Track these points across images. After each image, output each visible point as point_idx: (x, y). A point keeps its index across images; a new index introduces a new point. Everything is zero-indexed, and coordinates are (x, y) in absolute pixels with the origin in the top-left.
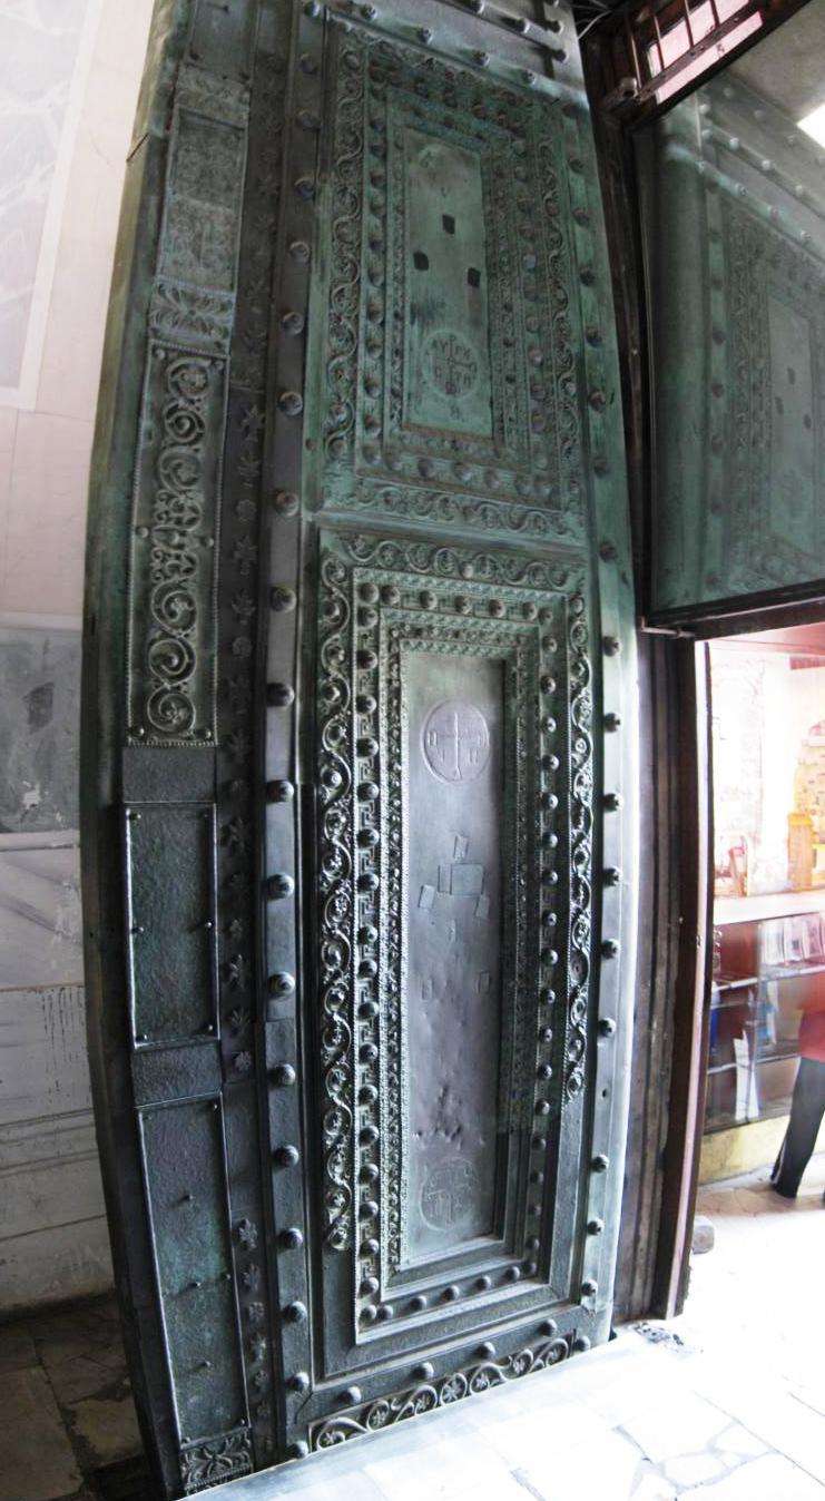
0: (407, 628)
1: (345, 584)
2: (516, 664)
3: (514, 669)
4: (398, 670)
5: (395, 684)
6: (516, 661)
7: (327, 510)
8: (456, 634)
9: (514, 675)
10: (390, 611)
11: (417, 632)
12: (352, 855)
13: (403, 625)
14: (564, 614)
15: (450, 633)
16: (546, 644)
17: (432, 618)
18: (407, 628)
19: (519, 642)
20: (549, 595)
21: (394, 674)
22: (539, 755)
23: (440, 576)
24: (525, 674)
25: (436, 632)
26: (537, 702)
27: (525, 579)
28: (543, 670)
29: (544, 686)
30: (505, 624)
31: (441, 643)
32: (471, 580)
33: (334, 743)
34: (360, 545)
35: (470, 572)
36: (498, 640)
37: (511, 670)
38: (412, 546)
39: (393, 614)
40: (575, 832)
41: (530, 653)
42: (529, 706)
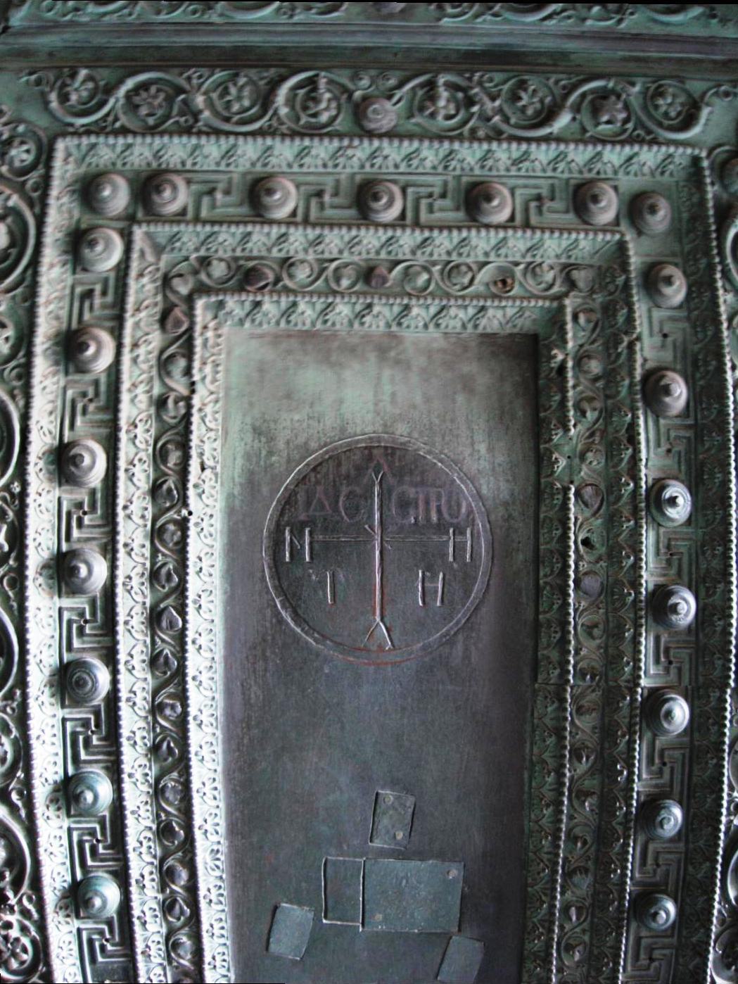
0: (219, 270)
1: (33, 178)
4: (188, 372)
5: (173, 411)
6: (563, 332)
7: (22, 33)
8: (368, 274)
9: (562, 368)
10: (163, 231)
13: (205, 262)
14: (702, 202)
15: (349, 271)
16: (652, 280)
17: (283, 237)
18: (219, 270)
19: (572, 284)
20: (649, 157)
21: (180, 387)
22: (635, 584)
23: (293, 134)
24: (595, 367)
25: (302, 274)
26: (633, 440)
27: (563, 121)
28: (648, 351)
29: (653, 389)
30: (518, 243)
31: (320, 303)
32: (391, 135)
34: (79, 90)
35: (386, 114)
36: (504, 281)
39: (174, 238)
41: (609, 310)
42: (612, 452)
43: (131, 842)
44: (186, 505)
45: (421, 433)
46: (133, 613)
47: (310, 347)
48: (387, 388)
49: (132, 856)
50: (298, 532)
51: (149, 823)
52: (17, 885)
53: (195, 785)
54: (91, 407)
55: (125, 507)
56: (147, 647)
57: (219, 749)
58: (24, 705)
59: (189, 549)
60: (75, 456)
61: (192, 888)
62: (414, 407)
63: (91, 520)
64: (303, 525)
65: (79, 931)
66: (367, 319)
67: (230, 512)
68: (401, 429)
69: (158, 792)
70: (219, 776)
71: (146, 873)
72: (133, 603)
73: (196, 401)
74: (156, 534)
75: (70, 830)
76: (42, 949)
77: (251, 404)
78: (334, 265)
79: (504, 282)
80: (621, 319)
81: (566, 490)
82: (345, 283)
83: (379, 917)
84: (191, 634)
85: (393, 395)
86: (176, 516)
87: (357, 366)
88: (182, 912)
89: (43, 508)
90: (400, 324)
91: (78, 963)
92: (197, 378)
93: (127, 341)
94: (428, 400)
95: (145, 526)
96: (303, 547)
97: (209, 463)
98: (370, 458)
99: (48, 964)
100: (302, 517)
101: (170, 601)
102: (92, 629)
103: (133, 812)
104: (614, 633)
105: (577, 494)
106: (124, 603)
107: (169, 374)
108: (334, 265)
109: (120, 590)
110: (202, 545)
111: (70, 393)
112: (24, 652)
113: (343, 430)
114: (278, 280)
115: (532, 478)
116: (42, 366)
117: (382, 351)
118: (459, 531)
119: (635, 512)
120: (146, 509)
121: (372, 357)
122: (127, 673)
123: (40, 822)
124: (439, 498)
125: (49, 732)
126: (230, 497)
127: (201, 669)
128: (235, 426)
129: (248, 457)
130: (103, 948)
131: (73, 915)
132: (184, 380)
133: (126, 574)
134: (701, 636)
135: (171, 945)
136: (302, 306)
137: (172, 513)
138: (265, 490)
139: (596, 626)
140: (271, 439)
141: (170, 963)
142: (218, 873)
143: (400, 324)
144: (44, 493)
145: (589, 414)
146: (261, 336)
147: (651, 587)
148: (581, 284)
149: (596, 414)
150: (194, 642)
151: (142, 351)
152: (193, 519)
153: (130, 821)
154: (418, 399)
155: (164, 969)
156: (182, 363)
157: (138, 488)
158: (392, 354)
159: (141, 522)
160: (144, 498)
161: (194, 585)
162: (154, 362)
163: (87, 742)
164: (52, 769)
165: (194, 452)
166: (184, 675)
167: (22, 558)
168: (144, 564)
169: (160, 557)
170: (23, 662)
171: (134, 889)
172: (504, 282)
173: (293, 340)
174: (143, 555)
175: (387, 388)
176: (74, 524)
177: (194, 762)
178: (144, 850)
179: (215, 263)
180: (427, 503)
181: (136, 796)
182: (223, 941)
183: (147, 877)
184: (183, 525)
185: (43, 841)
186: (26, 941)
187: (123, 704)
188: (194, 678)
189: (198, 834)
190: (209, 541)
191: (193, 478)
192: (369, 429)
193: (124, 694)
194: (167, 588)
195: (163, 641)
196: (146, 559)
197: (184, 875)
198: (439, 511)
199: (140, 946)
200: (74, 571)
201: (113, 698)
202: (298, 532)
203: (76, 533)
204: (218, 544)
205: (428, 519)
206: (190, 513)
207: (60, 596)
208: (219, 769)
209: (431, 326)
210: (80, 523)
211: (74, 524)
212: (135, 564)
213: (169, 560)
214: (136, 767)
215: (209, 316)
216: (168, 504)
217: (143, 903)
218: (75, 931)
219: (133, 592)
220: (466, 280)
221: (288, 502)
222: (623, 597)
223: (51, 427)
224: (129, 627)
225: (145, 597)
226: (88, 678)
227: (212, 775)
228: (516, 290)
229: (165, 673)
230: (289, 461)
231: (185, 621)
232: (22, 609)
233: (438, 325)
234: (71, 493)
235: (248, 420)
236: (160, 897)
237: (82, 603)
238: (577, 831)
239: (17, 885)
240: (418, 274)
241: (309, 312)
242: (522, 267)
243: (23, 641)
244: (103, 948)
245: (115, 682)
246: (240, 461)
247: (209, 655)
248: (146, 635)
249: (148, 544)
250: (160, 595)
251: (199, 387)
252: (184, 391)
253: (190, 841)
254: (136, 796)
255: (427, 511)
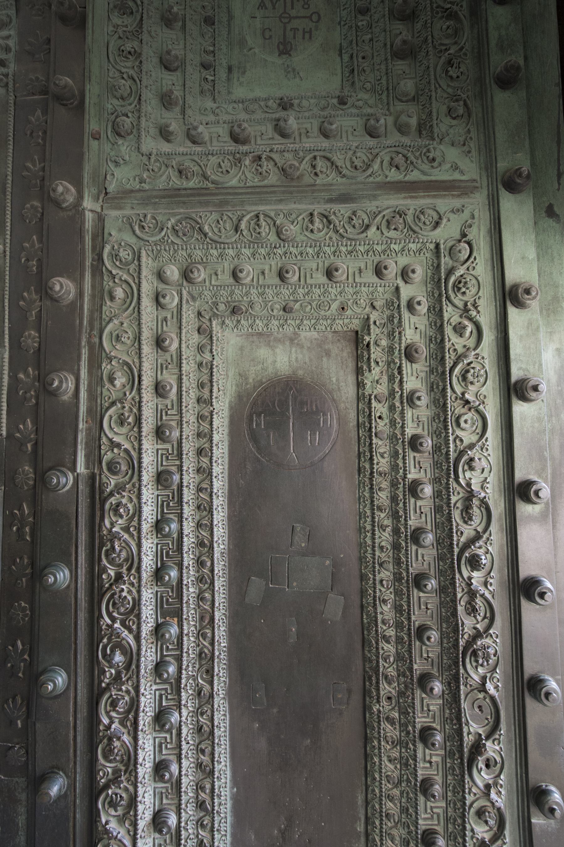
2: (369, 334)
3: (367, 338)
4: (211, 351)
6: (369, 330)
9: (368, 345)
11: (235, 311)
12: (139, 545)
13: (216, 304)
18: (222, 307)
21: (207, 356)
24: (384, 343)
25: (257, 308)
33: (124, 430)
37: (363, 340)
38: (215, 216)
40: (468, 531)
43: (185, 549)
44: (212, 405)
45: (308, 374)
47: (261, 340)
48: (294, 356)
49: (185, 555)
50: (259, 415)
51: (193, 540)
52: (129, 569)
53: (215, 522)
54: (170, 366)
55: (186, 407)
57: (226, 507)
58: (140, 490)
59: (214, 423)
60: (162, 386)
61: (212, 571)
62: (305, 363)
64: (262, 413)
65: (157, 592)
66: (285, 327)
67: (231, 408)
68: (300, 372)
69: (199, 525)
70: (226, 519)
71: (191, 563)
73: (215, 363)
74: (200, 417)
75: (157, 544)
76: (137, 603)
77: (238, 364)
78: (270, 304)
79: (343, 308)
80: (396, 321)
81: (370, 395)
82: (275, 311)
83: (295, 584)
84: (214, 459)
85: (297, 358)
87: (281, 347)
88: (206, 582)
90: (299, 328)
91: (154, 608)
92: (215, 353)
93: (183, 338)
94: (311, 360)
96: (261, 422)
97: (222, 388)
98: (288, 385)
99: (139, 610)
100: (260, 410)
101: (206, 445)
103: (186, 536)
104: (395, 455)
105: (375, 397)
106: (186, 447)
107: (202, 352)
108: (270, 304)
109: (184, 441)
111: (159, 361)
112: (140, 467)
113: (276, 374)
114: (247, 311)
115: (356, 392)
116: (147, 349)
117: (292, 340)
118: (325, 414)
119: (402, 403)
121: (288, 343)
123: (144, 541)
124: (316, 401)
125: (150, 500)
126: (230, 402)
128: (231, 374)
129: (237, 385)
130: (167, 600)
131: (155, 584)
132: (209, 354)
134: (435, 455)
135: (200, 598)
136: (257, 321)
138: (245, 399)
139: (385, 452)
140: (247, 379)
141: (199, 608)
142: (223, 563)
143: (299, 328)
145: (380, 364)
146: (241, 336)
147: (410, 436)
148: (378, 308)
149: (384, 363)
150: (216, 462)
151: (190, 342)
152: (215, 411)
153: (185, 539)
154: (307, 360)
155: (196, 611)
156: (209, 347)
157: (191, 399)
158: (296, 341)
161: (216, 438)
162: (196, 347)
163: (168, 505)
164: (150, 517)
165: (214, 384)
166: (212, 476)
167: (140, 428)
170: (140, 472)
171: (184, 571)
172: (343, 308)
173: (255, 337)
175: (294, 356)
177: (215, 512)
178: (190, 553)
179: (220, 304)
180: (311, 402)
181: (188, 527)
182: (224, 596)
183: (191, 566)
184: (211, 413)
185: (144, 549)
186: (129, 598)
187: (184, 488)
188: (216, 477)
189: (215, 545)
190: (222, 420)
191: (215, 395)
192: (287, 373)
193: (185, 484)
197: (209, 564)
198: (316, 406)
199: (185, 599)
200: (163, 433)
201: (180, 486)
202: (259, 415)
203: (164, 418)
204: (226, 422)
205: (312, 409)
208: (226, 515)
209: (312, 329)
210: (167, 414)
215: (219, 327)
217: (188, 578)
218: (154, 592)
220: (327, 308)
221: (254, 403)
222: (397, 440)
223: (152, 374)
227: (222, 518)
228: (349, 312)
230: (254, 387)
231: (212, 453)
232: (140, 449)
233: (315, 329)
235: (237, 370)
236: (197, 575)
238: (383, 544)
239: (129, 569)
240: (306, 306)
241: (260, 324)
242: (351, 301)
243: (140, 463)
244: (167, 600)
245: (181, 479)
246: (234, 387)
247: (222, 467)
249: (196, 421)
251: (216, 357)
252: (211, 359)
253: (212, 548)
254: (188, 527)
255: (311, 406)
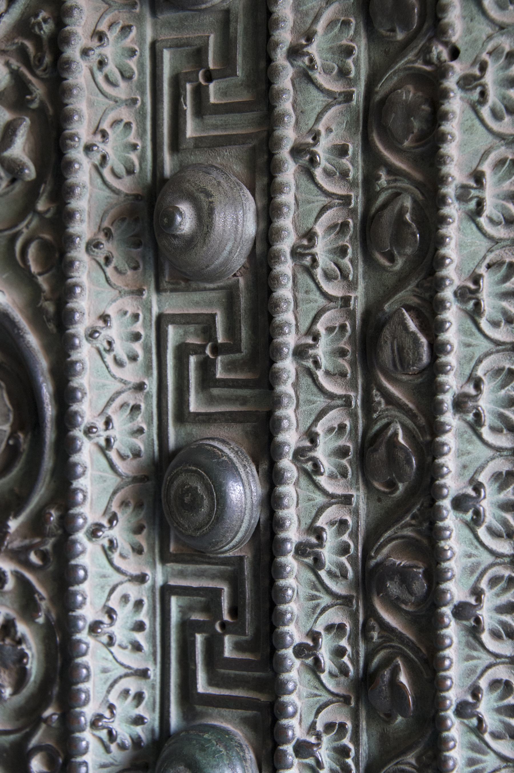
46: (320, 327)
56: (353, 416)
63: (224, 93)
72: (322, 302)
86: (419, 65)
89: (111, 68)
95: (348, 97)
102: (229, 367)
110: (490, 139)
120: (348, 51)
122: (304, 482)
127: (483, 478)
133: (302, 231)
137: (410, 56)
144: (112, 36)
159: (336, 87)
160: (346, 24)
168: (346, 200)
169: (384, 179)
174: (344, 174)
176: (188, 107)
194: (400, 263)
195: (390, 399)
196: (353, 185)
206: (455, 53)
207: (159, 290)
211: (188, 107)
212: (323, 200)
213: (404, 184)
214: (319, 727)
216: (400, 36)
219: (319, 272)
224: (309, 364)
225: (352, 285)
226: (200, 489)
229: (392, 485)
234: (181, 26)
237: (210, 304)
248: (355, 388)
250: (389, 280)
